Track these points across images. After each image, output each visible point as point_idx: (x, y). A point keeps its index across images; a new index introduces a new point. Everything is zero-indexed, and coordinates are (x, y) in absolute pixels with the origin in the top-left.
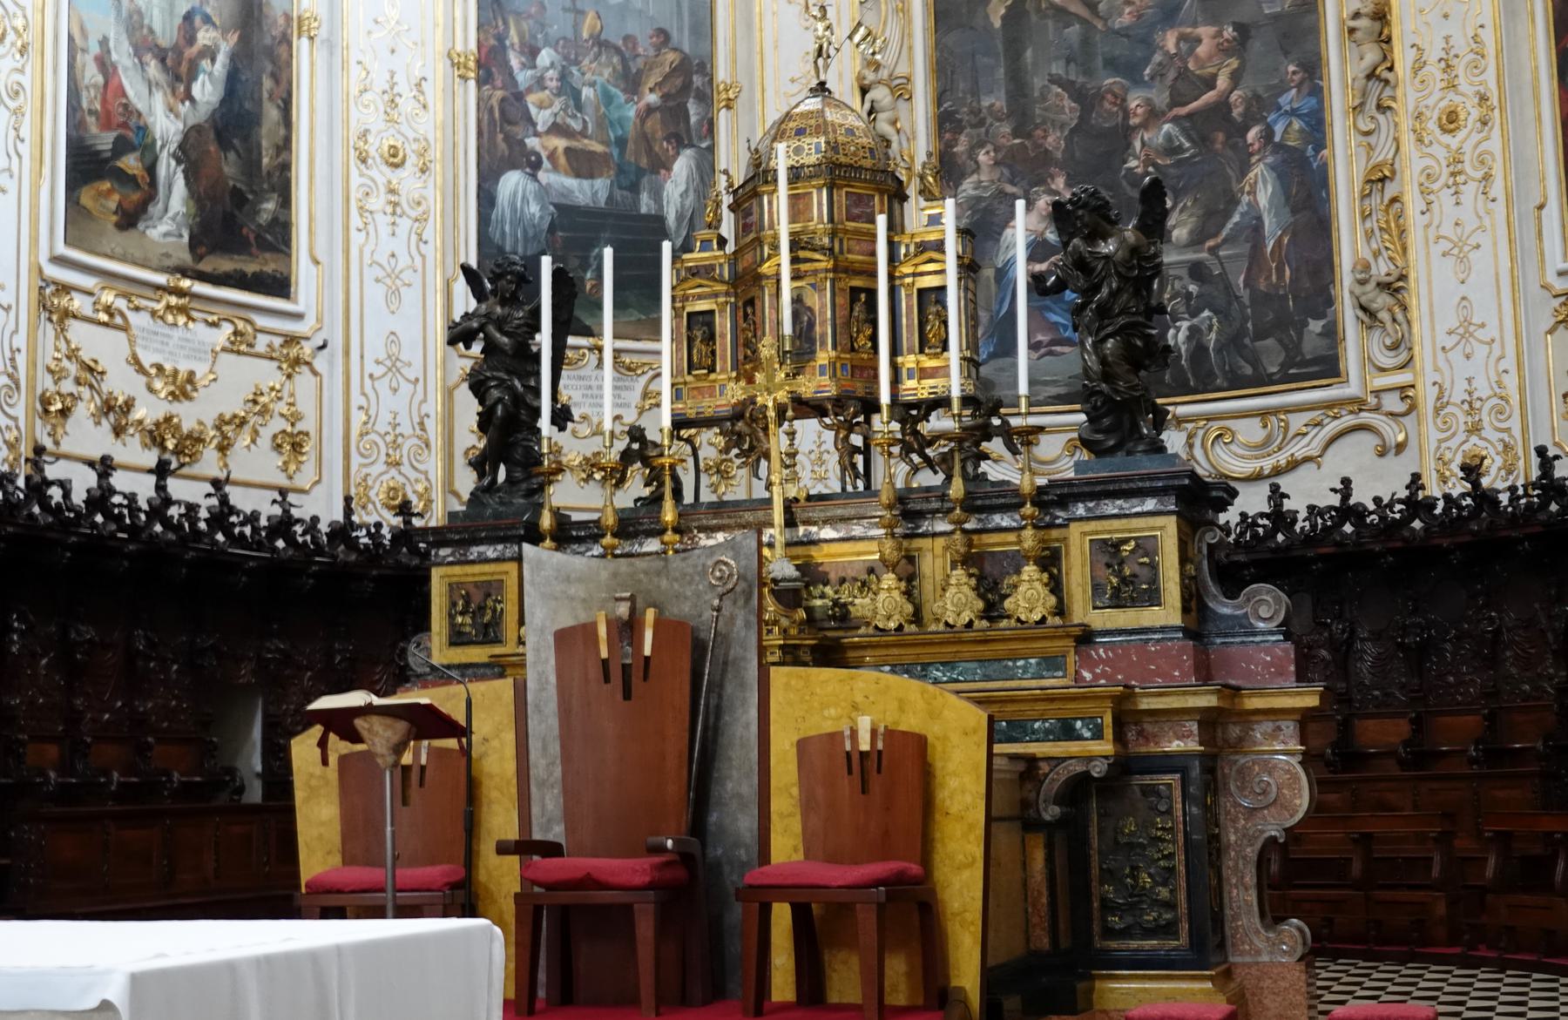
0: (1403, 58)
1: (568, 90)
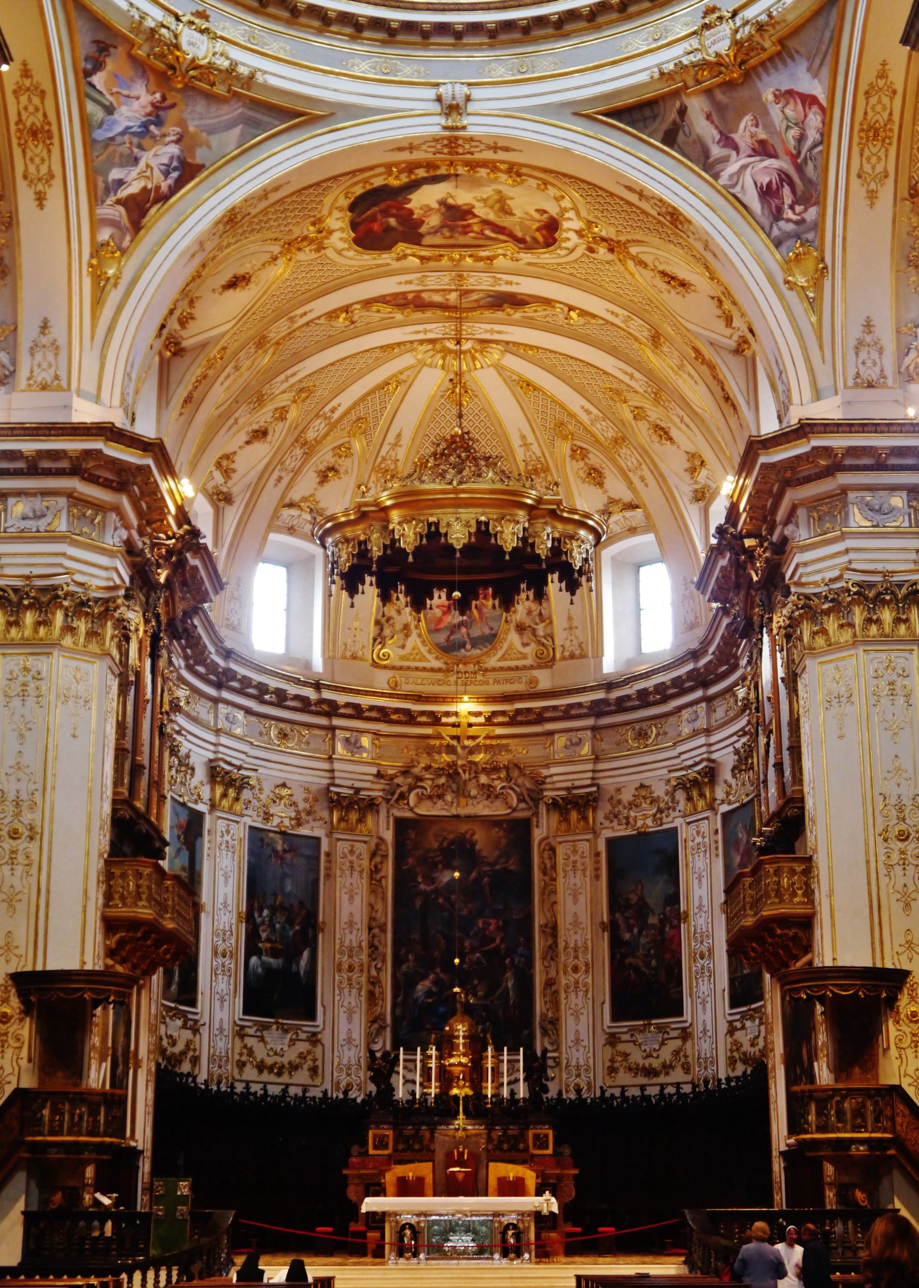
0: (561, 945)
1: (272, 925)
